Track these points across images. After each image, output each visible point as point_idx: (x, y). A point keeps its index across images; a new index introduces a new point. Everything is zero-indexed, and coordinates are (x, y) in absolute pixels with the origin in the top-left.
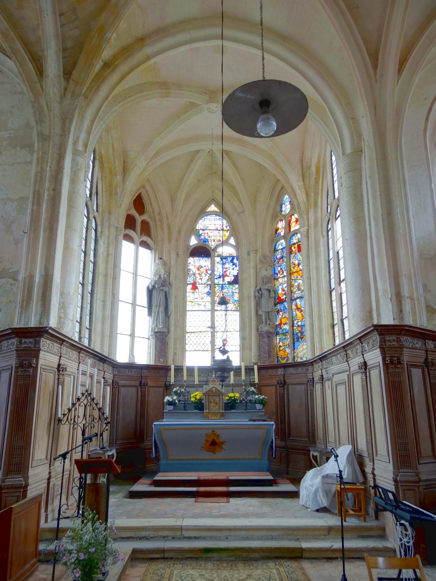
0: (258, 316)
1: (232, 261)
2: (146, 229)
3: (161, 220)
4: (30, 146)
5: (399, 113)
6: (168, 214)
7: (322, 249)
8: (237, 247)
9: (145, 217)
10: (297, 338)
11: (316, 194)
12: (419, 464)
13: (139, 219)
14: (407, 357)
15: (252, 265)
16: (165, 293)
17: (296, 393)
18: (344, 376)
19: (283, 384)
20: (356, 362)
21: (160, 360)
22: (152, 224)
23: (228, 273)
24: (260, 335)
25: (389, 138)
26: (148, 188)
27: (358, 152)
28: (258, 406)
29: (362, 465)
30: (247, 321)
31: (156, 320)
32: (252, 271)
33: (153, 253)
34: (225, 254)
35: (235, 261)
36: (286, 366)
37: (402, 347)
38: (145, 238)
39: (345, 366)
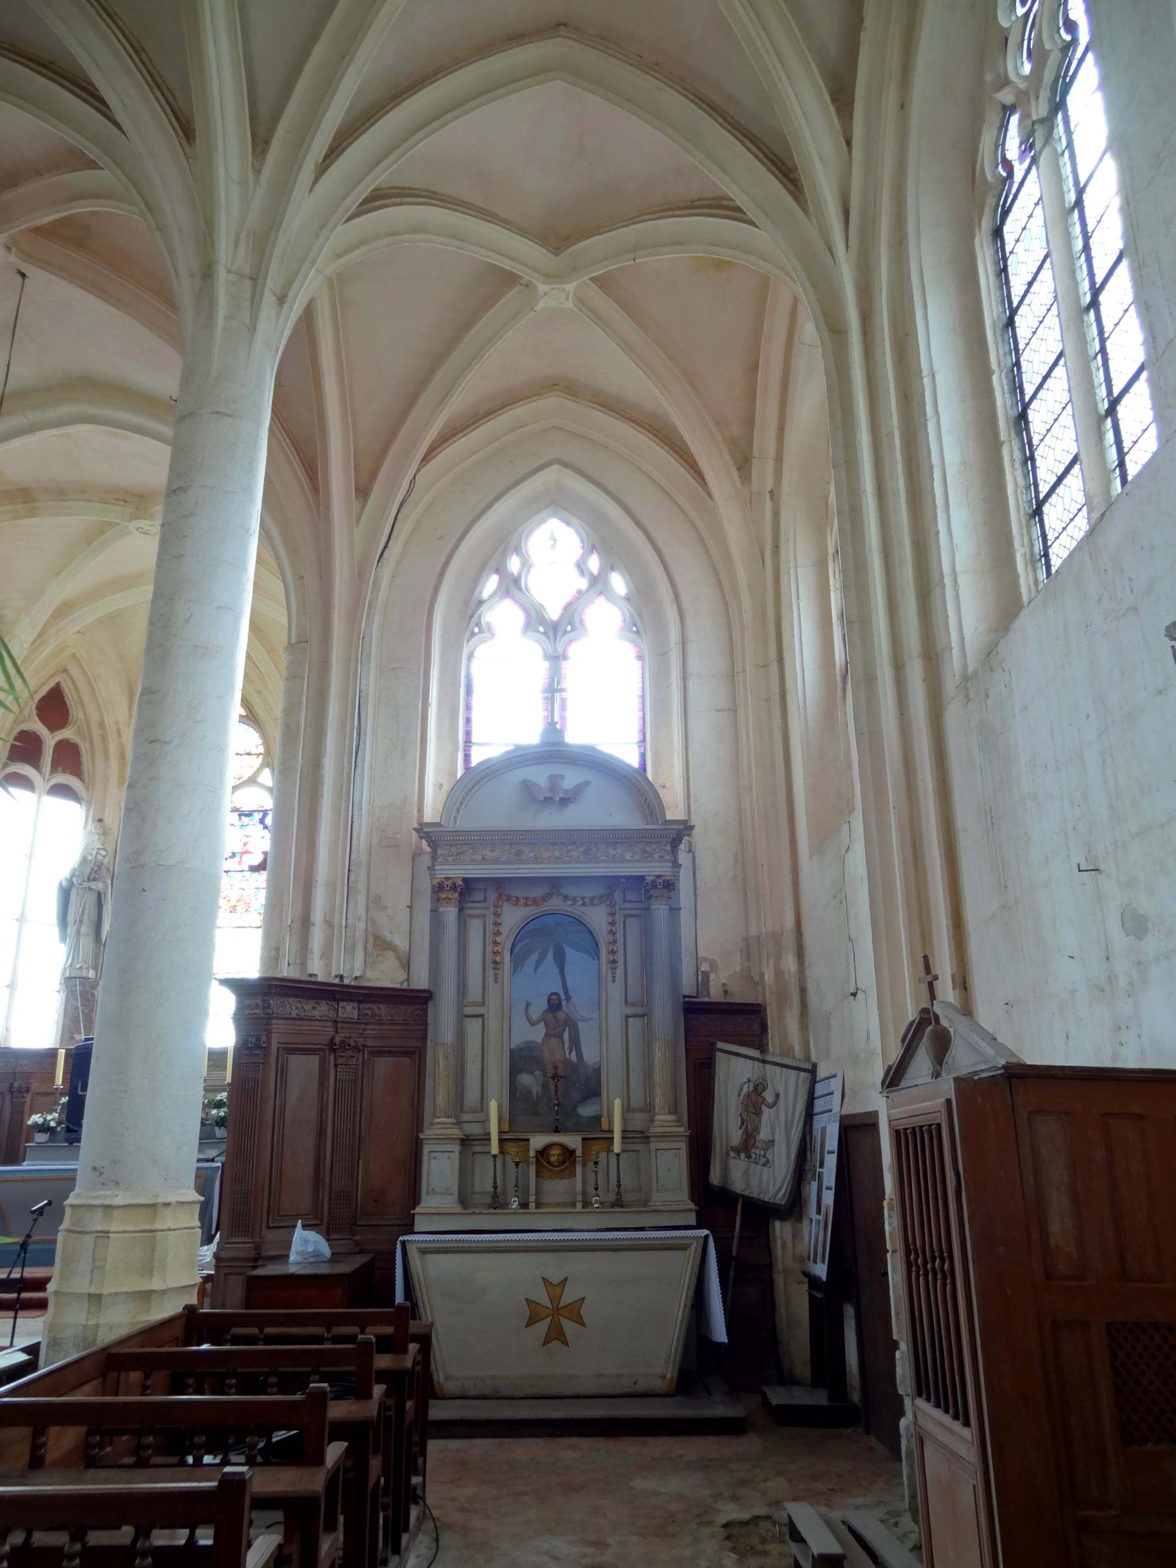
1: (262, 821)
2: (69, 758)
3: (104, 739)
6: (121, 727)
9: (65, 734)
12: (269, 1227)
13: (50, 740)
16: (99, 894)
21: (73, 1038)
22: (84, 748)
23: (250, 847)
26: (74, 670)
31: (74, 951)
33: (84, 808)
34: (246, 808)
35: (269, 821)
38: (62, 778)
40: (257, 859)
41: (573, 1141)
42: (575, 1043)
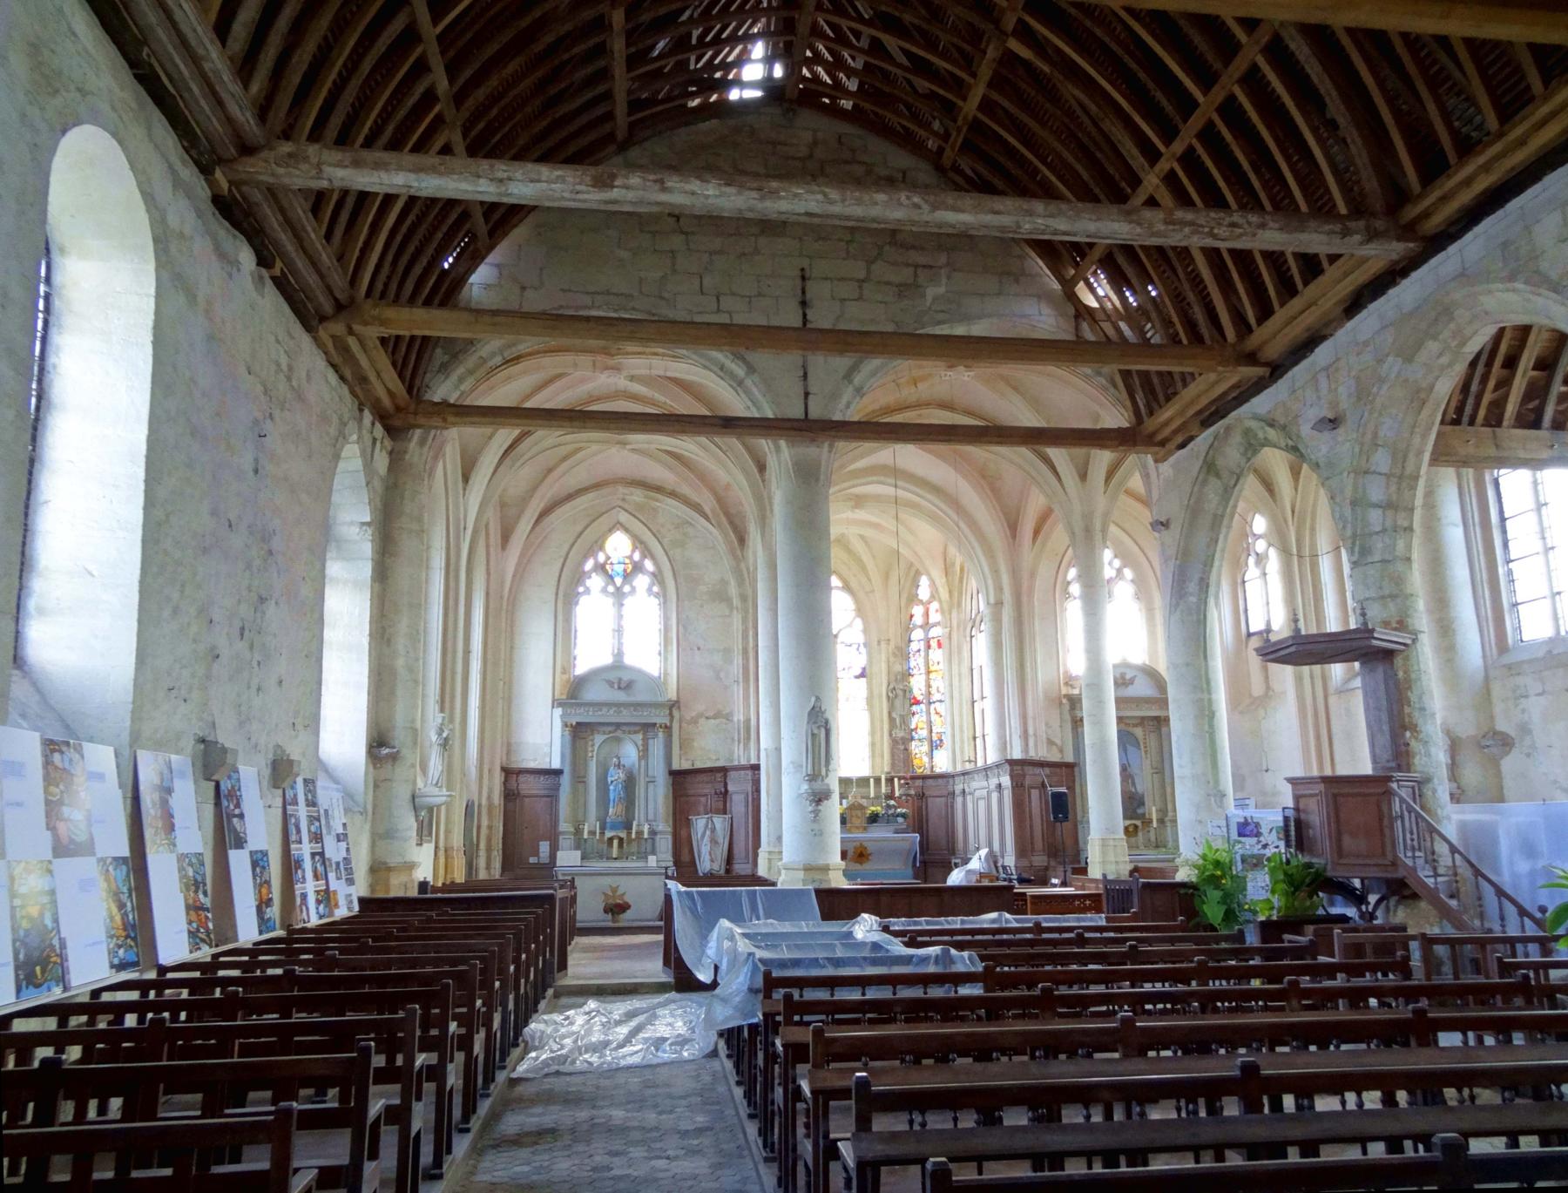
0: (892, 720)
4: (727, 600)
5: (1033, 575)
7: (966, 654)
8: (865, 631)
10: (934, 745)
11: (960, 594)
14: (1028, 782)
15: (884, 657)
17: (936, 805)
18: (985, 792)
19: (922, 796)
20: (994, 782)
24: (894, 742)
25: (1025, 599)
27: (999, 604)
28: (900, 820)
29: (995, 863)
30: (878, 724)
32: (884, 666)
36: (924, 778)
37: (1024, 776)
39: (985, 784)
40: (859, 672)
41: (1138, 823)
42: (1134, 784)
